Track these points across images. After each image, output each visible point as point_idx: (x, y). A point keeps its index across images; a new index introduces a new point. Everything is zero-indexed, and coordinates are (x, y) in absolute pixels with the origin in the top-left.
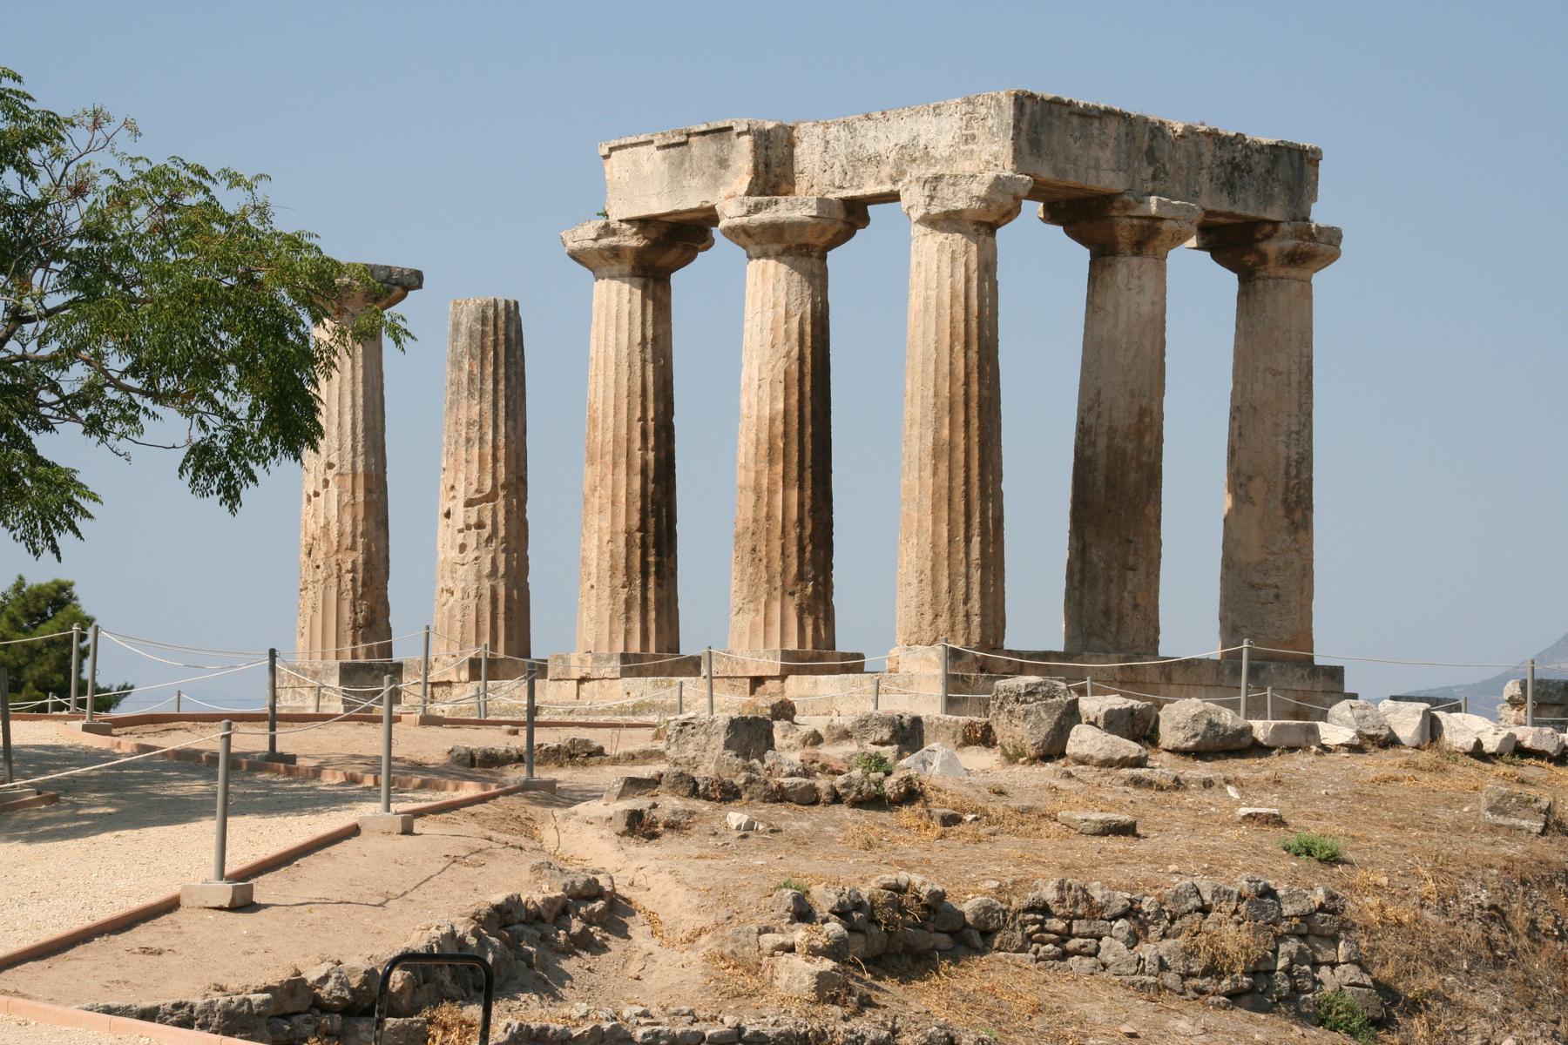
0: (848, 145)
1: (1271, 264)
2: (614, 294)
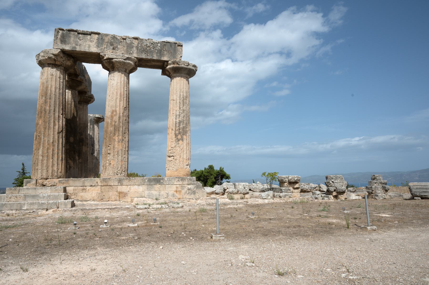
1: (171, 73)
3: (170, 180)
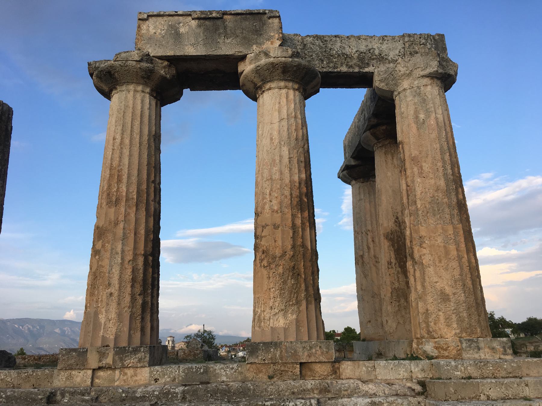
0: (321, 48)
2: (139, 102)
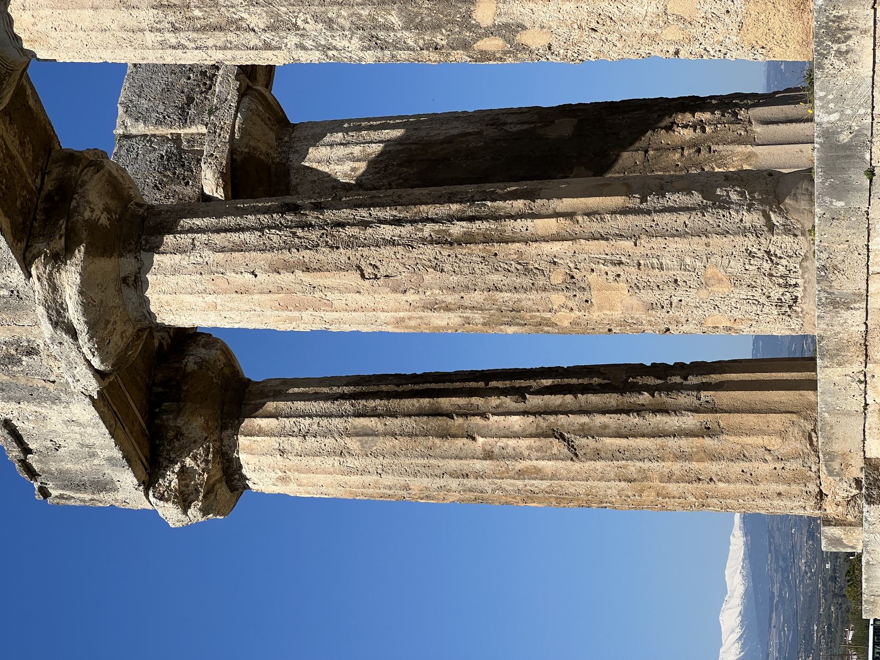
3: (841, 98)
